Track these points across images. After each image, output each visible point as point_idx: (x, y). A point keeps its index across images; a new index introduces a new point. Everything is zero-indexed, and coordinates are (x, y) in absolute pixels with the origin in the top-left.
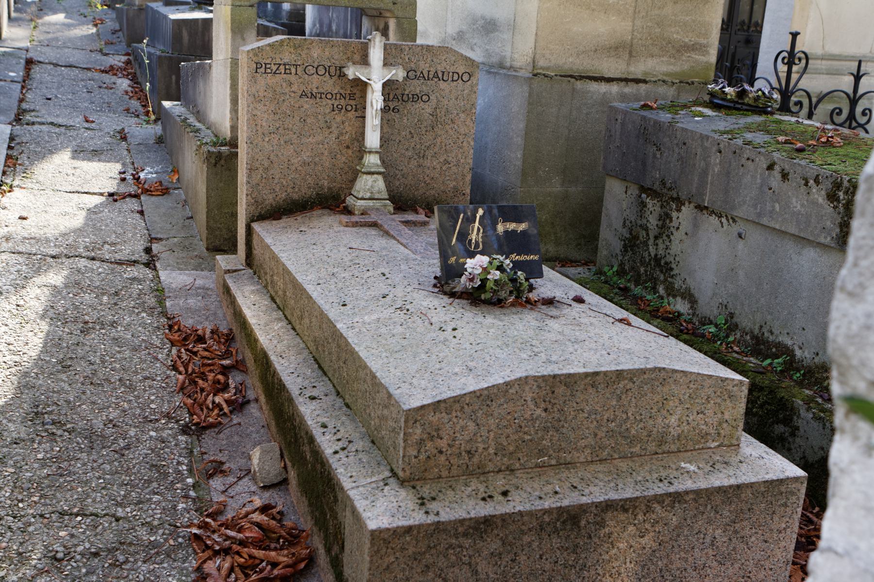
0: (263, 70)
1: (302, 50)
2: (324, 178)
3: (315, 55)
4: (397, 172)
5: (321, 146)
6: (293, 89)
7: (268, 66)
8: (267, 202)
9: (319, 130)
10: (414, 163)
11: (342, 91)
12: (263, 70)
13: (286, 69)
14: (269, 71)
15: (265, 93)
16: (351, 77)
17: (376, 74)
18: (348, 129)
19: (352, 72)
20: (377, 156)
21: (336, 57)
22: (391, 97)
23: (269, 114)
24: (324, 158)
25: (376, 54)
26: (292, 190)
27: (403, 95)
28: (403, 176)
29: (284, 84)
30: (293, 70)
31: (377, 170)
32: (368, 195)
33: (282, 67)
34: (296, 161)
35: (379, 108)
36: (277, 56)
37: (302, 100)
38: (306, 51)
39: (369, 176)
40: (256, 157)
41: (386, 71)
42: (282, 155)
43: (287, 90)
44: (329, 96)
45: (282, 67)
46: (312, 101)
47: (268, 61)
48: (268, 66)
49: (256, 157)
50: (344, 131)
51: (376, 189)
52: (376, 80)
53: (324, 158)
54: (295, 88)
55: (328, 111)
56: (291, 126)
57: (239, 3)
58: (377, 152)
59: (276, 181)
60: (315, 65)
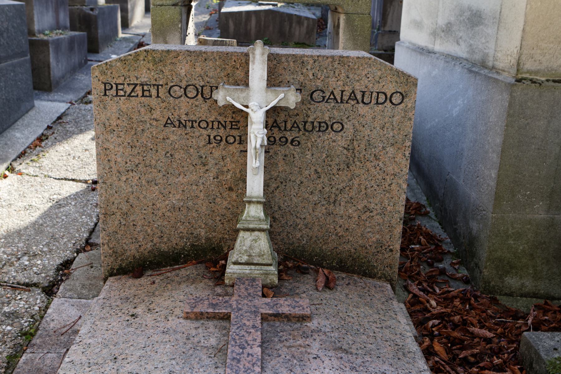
0: (113, 92)
1: (165, 66)
2: (200, 227)
3: (183, 72)
4: (298, 221)
5: (194, 187)
6: (154, 116)
7: (120, 87)
8: (128, 253)
9: (192, 168)
10: (321, 211)
11: (220, 119)
12: (113, 92)
13: (143, 91)
14: (121, 93)
15: (119, 122)
16: (221, 103)
17: (257, 100)
18: (231, 166)
19: (223, 96)
20: (260, 207)
21: (211, 74)
22: (289, 126)
23: (125, 147)
24: (200, 202)
25: (258, 71)
26: (159, 240)
27: (305, 123)
28: (306, 226)
29: (142, 110)
30: (154, 92)
31: (257, 226)
32: (245, 258)
33: (139, 88)
34: (163, 205)
35: (258, 146)
36: (132, 74)
37: (167, 129)
38: (169, 67)
39: (248, 233)
40: (112, 200)
41: (270, 95)
42: (145, 197)
43: (146, 118)
44: (203, 125)
45: (139, 88)
46: (180, 131)
47: (120, 81)
48: (120, 87)
49: (112, 200)
50: (225, 169)
51: (257, 250)
52: (255, 108)
53: (200, 202)
54: (157, 114)
55: (202, 144)
56: (154, 162)
57: (161, 3)
58: (258, 202)
59: (138, 229)
60: (183, 84)
